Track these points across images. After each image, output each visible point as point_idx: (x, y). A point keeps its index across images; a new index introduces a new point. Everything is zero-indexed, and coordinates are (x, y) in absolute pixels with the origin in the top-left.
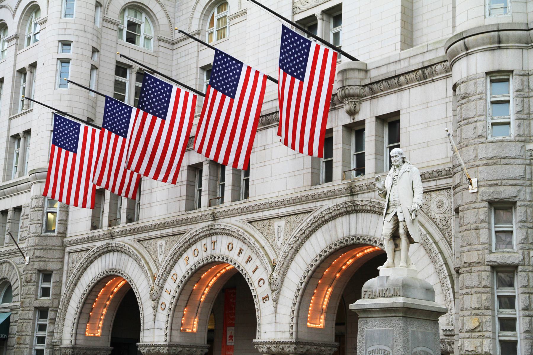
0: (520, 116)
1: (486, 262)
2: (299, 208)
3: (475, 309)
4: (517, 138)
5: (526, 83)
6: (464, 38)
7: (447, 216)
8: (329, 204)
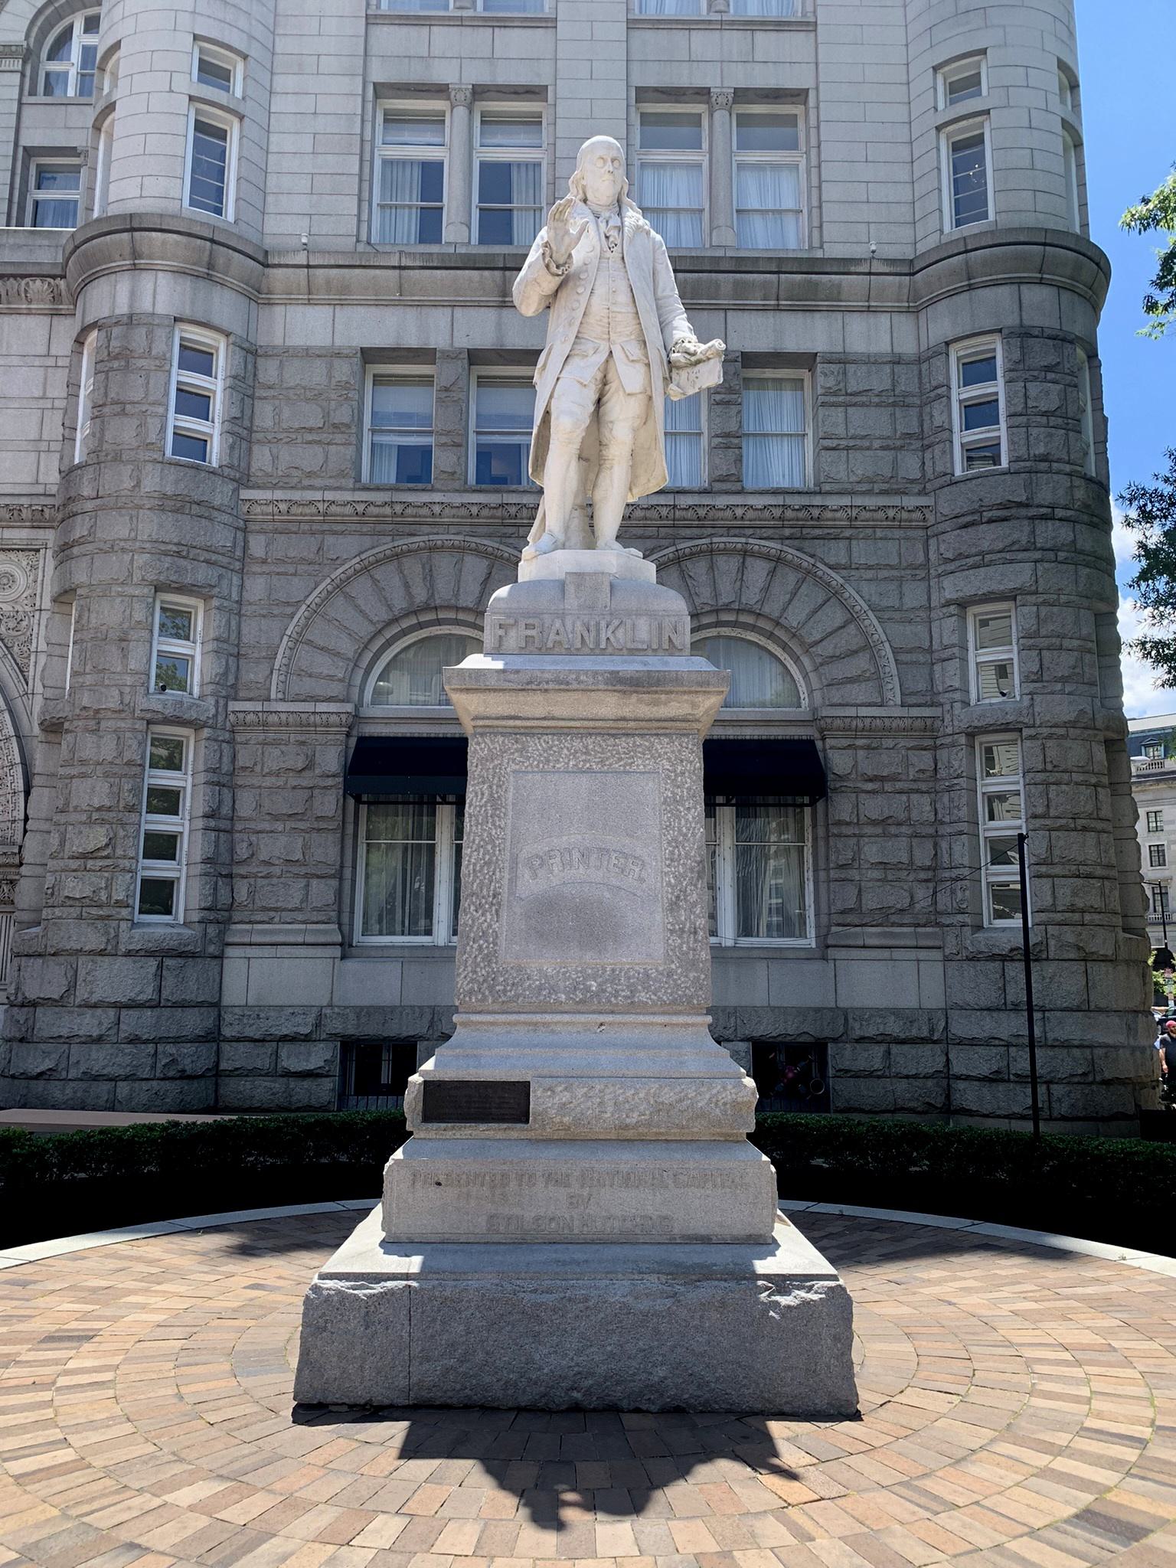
0: (236, 429)
1: (138, 713)
3: (99, 809)
4: (227, 471)
5: (250, 367)
6: (133, 230)
7: (20, 609)
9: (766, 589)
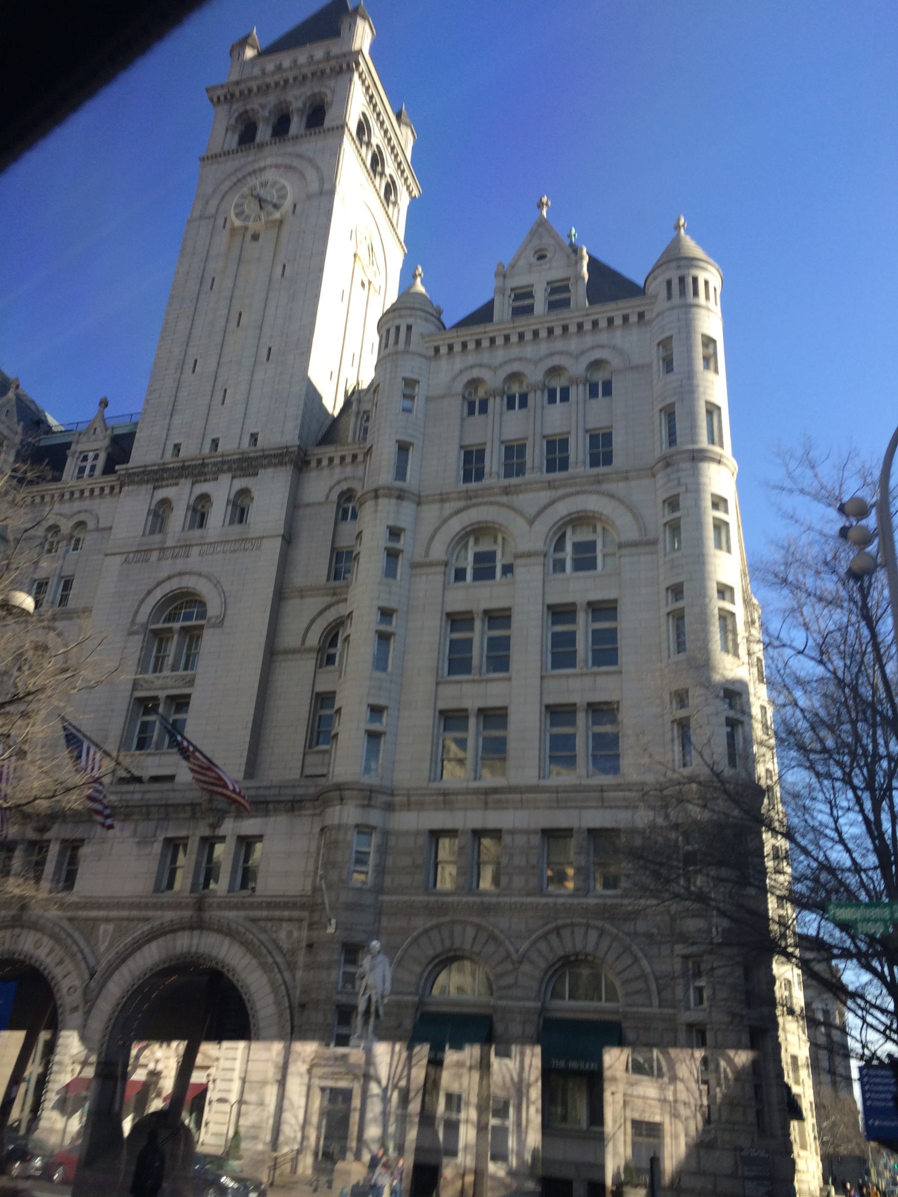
2: (135, 913)
8: (169, 915)
9: (597, 944)
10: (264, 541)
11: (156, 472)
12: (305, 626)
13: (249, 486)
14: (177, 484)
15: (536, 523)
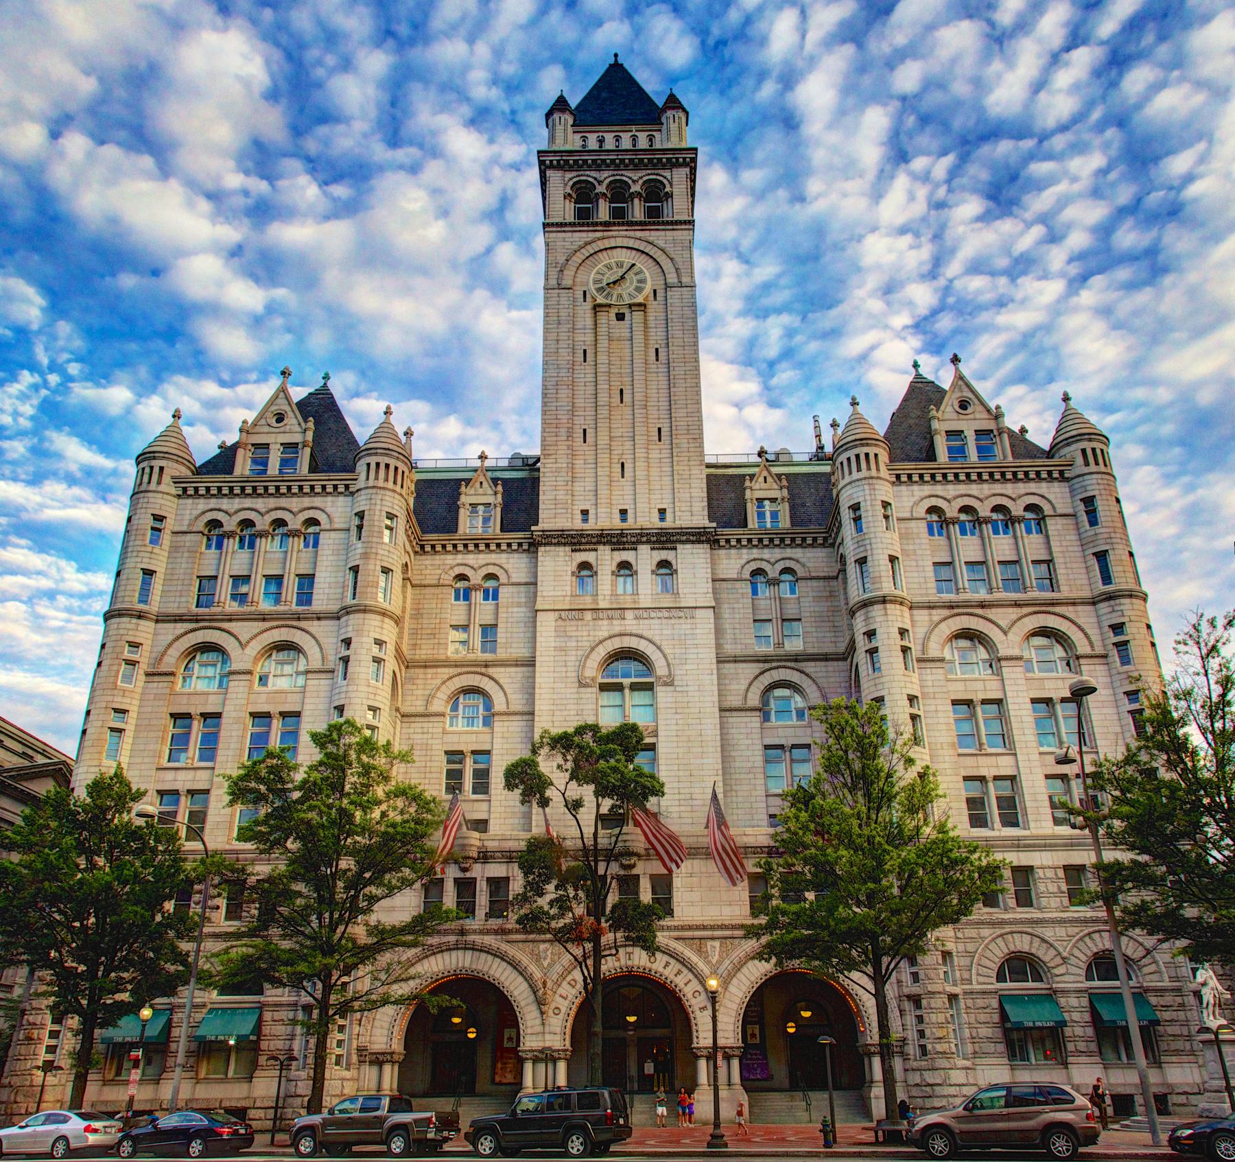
10: (698, 611)
11: (572, 537)
12: (744, 687)
13: (669, 559)
14: (596, 550)
15: (1010, 635)
